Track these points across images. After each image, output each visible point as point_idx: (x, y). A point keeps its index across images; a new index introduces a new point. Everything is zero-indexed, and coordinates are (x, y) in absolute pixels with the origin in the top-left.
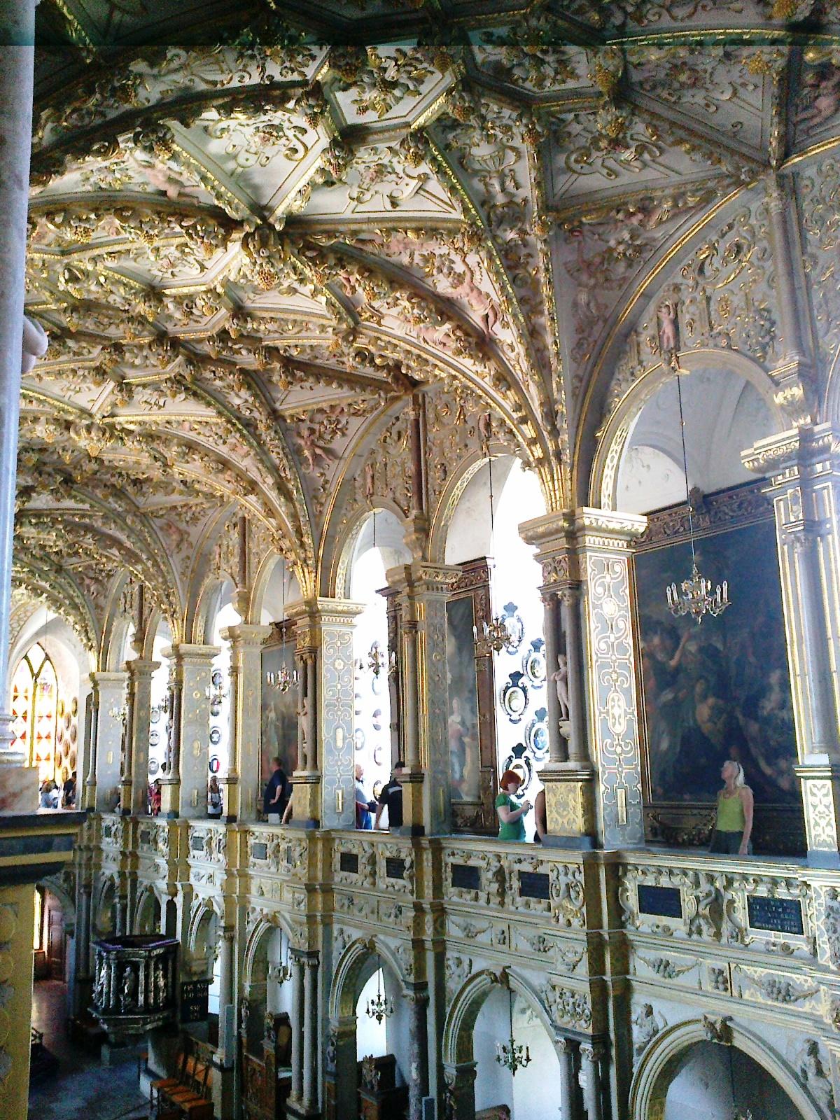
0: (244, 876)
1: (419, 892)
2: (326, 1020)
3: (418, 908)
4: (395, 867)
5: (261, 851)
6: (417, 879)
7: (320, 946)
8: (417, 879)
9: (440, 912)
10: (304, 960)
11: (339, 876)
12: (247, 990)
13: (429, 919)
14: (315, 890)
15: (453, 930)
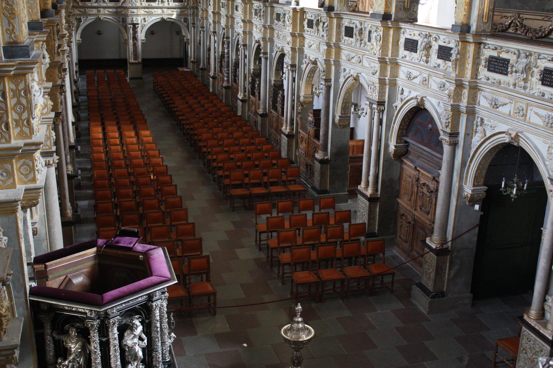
0: (339, 49)
1: (461, 73)
2: (387, 146)
3: (459, 85)
4: (444, 53)
5: (349, 32)
6: (460, 63)
7: (386, 100)
8: (460, 63)
9: (475, 89)
10: (375, 106)
11: (402, 52)
12: (337, 118)
13: (466, 92)
14: (386, 62)
15: (483, 102)
